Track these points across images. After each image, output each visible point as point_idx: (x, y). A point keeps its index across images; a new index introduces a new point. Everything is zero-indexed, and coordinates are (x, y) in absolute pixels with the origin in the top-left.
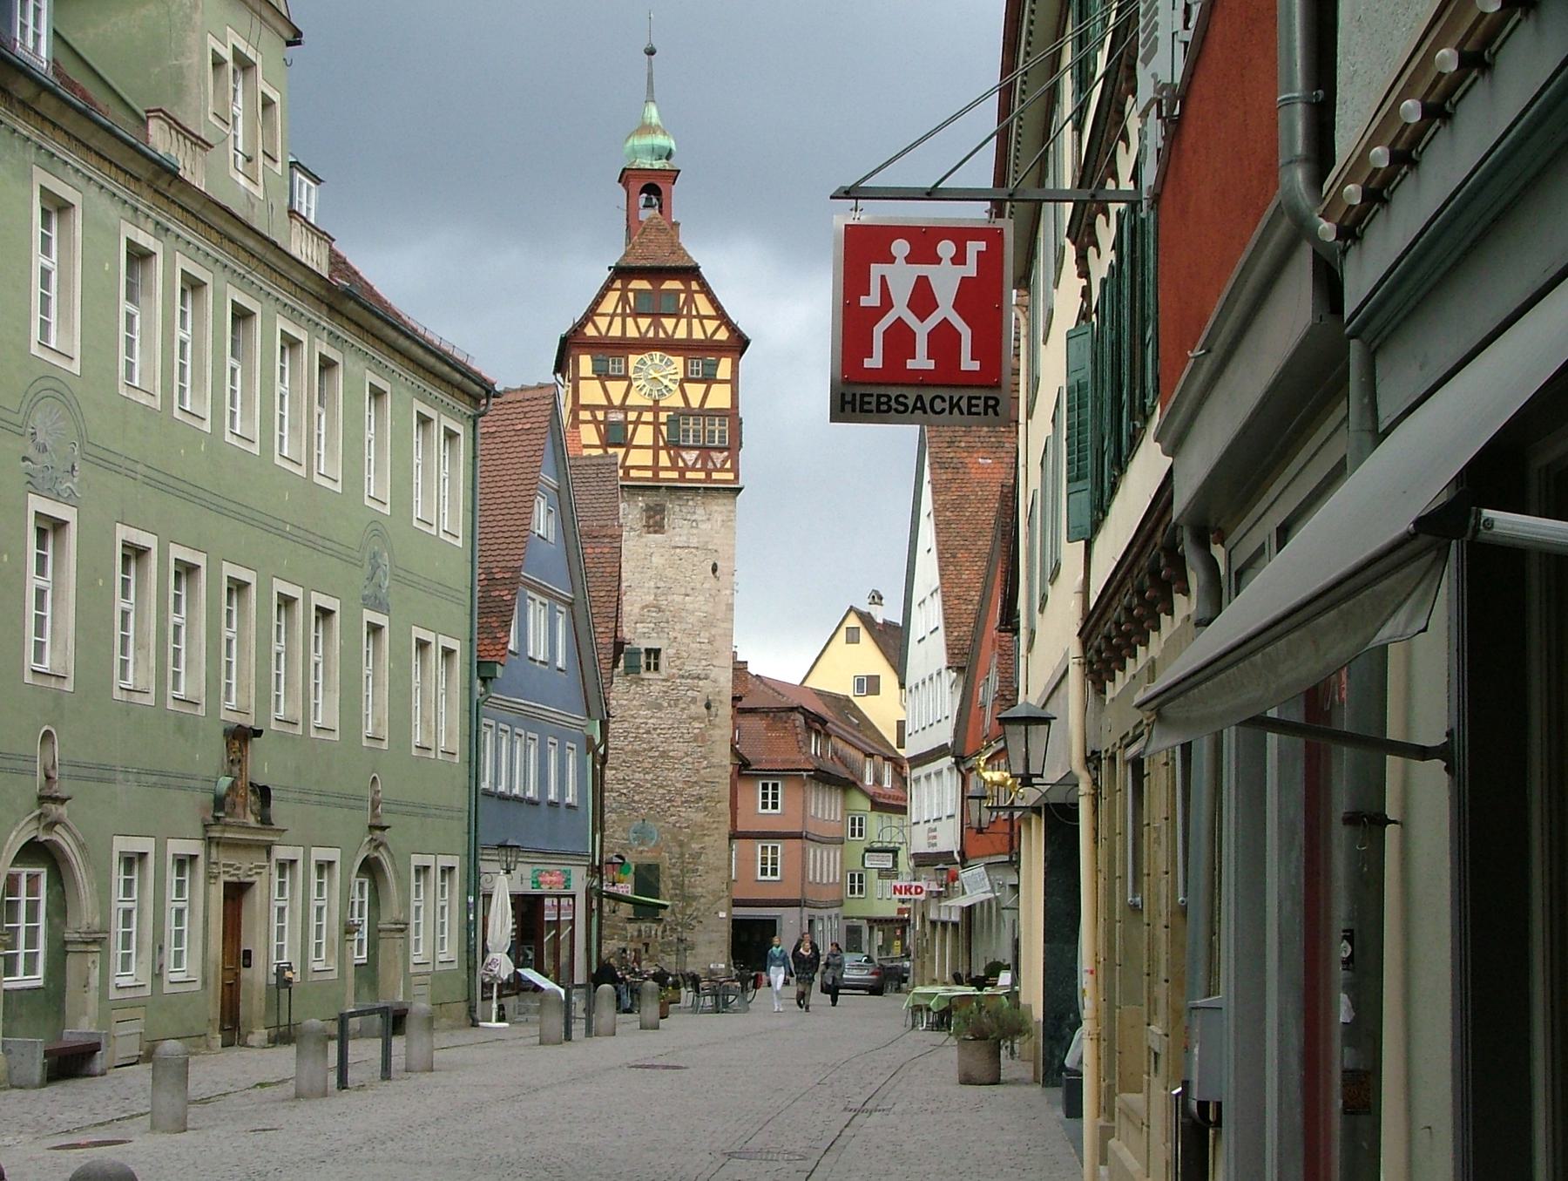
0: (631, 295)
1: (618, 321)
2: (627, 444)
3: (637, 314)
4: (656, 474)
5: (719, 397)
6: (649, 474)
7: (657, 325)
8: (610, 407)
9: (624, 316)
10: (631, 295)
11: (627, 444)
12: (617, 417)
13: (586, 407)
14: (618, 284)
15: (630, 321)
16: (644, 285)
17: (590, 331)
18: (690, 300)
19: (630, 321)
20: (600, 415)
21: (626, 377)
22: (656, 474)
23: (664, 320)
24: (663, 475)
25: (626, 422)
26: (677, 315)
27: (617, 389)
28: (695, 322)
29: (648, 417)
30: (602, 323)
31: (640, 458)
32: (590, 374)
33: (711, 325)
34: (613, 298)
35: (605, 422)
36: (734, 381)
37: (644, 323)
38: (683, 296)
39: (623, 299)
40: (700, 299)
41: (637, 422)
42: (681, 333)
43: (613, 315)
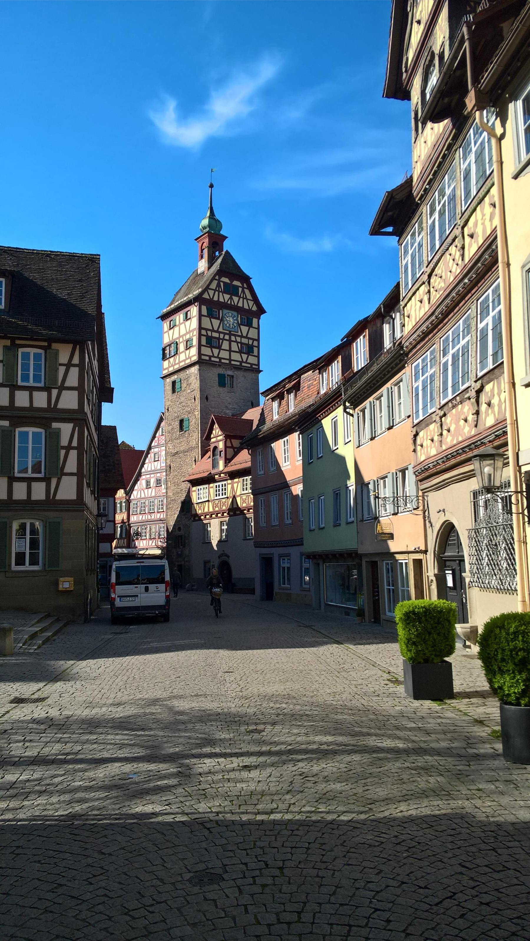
0: (222, 284)
1: (217, 293)
2: (219, 348)
3: (225, 292)
4: (230, 362)
5: (253, 333)
6: (227, 362)
7: (231, 298)
8: (213, 331)
9: (219, 292)
10: (222, 284)
11: (219, 348)
12: (215, 335)
13: (204, 329)
14: (217, 277)
15: (221, 294)
16: (227, 280)
17: (206, 296)
18: (243, 291)
19: (221, 294)
20: (209, 333)
21: (218, 318)
22: (230, 362)
23: (233, 297)
24: (233, 362)
25: (219, 339)
26: (237, 295)
27: (216, 323)
28: (245, 300)
29: (227, 337)
30: (211, 293)
31: (224, 354)
32: (206, 314)
33: (251, 303)
34: (215, 283)
35: (212, 337)
36: (258, 328)
37: (227, 297)
38: (240, 289)
39: (218, 285)
40: (247, 291)
41: (224, 339)
42: (240, 305)
43: (215, 290)
